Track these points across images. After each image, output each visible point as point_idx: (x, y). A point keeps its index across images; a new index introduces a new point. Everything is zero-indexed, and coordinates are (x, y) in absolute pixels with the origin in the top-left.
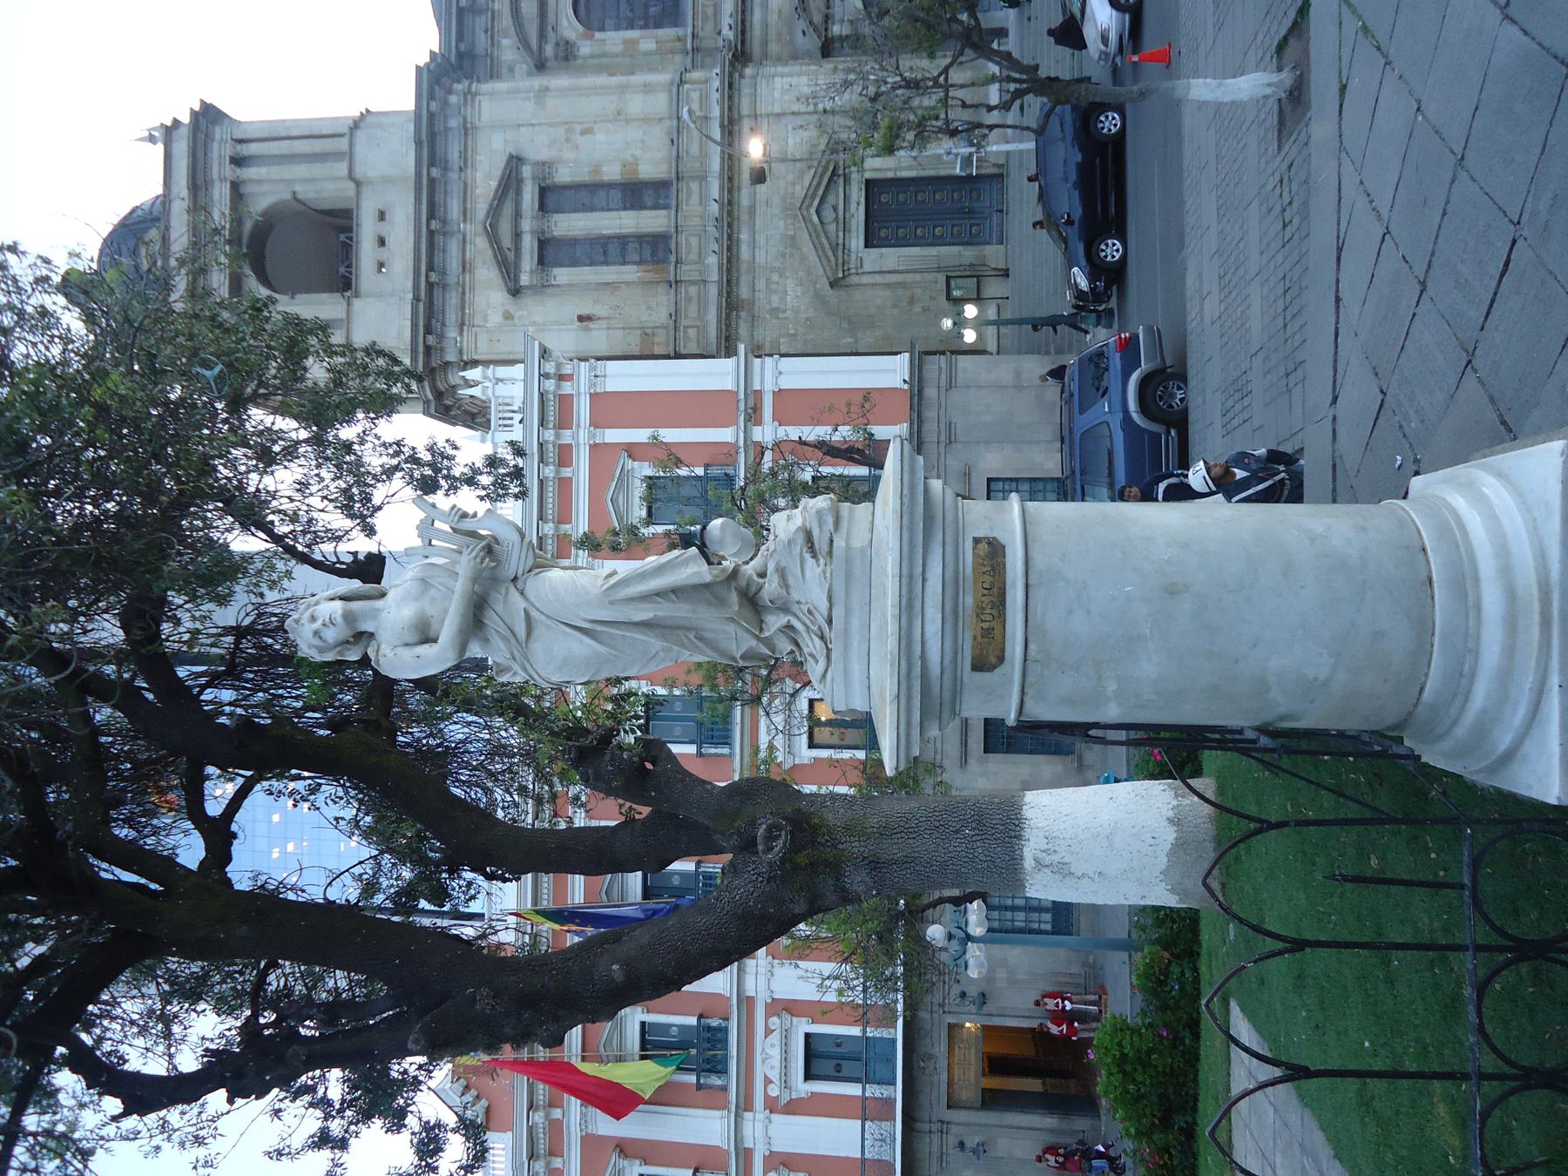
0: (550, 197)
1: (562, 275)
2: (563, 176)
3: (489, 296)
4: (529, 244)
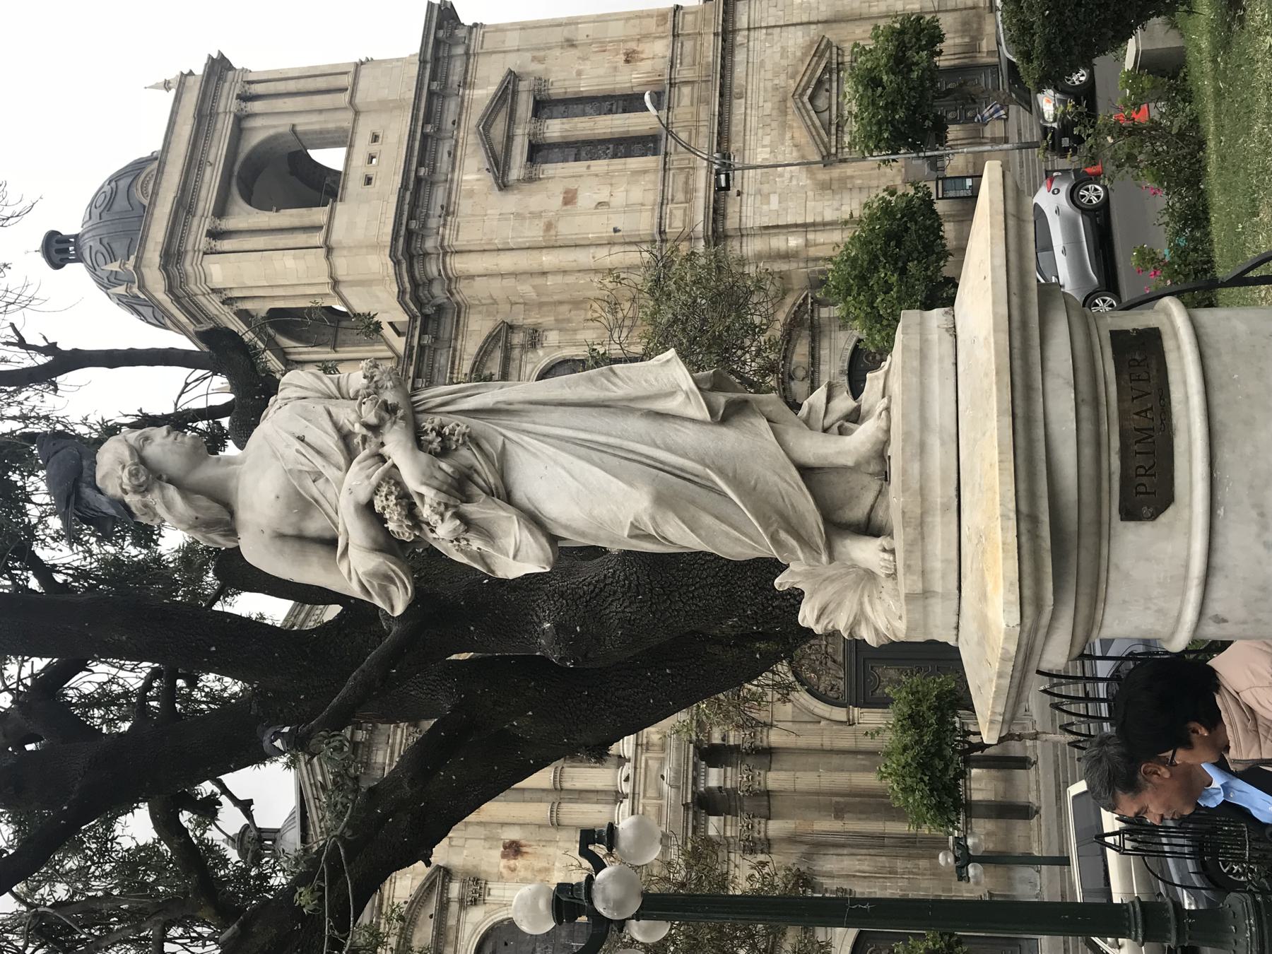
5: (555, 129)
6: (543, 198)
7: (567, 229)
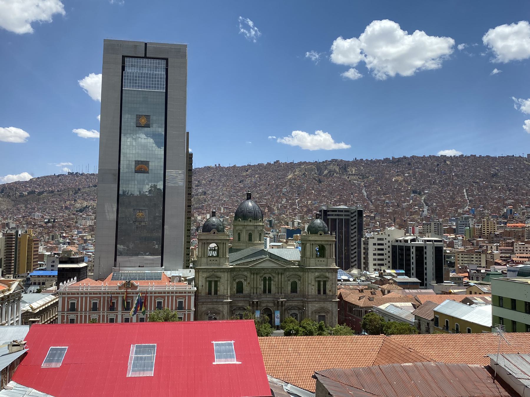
0: (216, 282)
1: (207, 283)
2: (218, 283)
3: (205, 275)
4: (211, 279)
5: (322, 283)
6: (313, 283)
7: (309, 285)
